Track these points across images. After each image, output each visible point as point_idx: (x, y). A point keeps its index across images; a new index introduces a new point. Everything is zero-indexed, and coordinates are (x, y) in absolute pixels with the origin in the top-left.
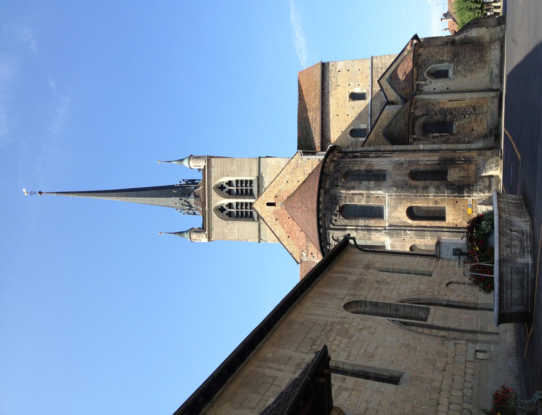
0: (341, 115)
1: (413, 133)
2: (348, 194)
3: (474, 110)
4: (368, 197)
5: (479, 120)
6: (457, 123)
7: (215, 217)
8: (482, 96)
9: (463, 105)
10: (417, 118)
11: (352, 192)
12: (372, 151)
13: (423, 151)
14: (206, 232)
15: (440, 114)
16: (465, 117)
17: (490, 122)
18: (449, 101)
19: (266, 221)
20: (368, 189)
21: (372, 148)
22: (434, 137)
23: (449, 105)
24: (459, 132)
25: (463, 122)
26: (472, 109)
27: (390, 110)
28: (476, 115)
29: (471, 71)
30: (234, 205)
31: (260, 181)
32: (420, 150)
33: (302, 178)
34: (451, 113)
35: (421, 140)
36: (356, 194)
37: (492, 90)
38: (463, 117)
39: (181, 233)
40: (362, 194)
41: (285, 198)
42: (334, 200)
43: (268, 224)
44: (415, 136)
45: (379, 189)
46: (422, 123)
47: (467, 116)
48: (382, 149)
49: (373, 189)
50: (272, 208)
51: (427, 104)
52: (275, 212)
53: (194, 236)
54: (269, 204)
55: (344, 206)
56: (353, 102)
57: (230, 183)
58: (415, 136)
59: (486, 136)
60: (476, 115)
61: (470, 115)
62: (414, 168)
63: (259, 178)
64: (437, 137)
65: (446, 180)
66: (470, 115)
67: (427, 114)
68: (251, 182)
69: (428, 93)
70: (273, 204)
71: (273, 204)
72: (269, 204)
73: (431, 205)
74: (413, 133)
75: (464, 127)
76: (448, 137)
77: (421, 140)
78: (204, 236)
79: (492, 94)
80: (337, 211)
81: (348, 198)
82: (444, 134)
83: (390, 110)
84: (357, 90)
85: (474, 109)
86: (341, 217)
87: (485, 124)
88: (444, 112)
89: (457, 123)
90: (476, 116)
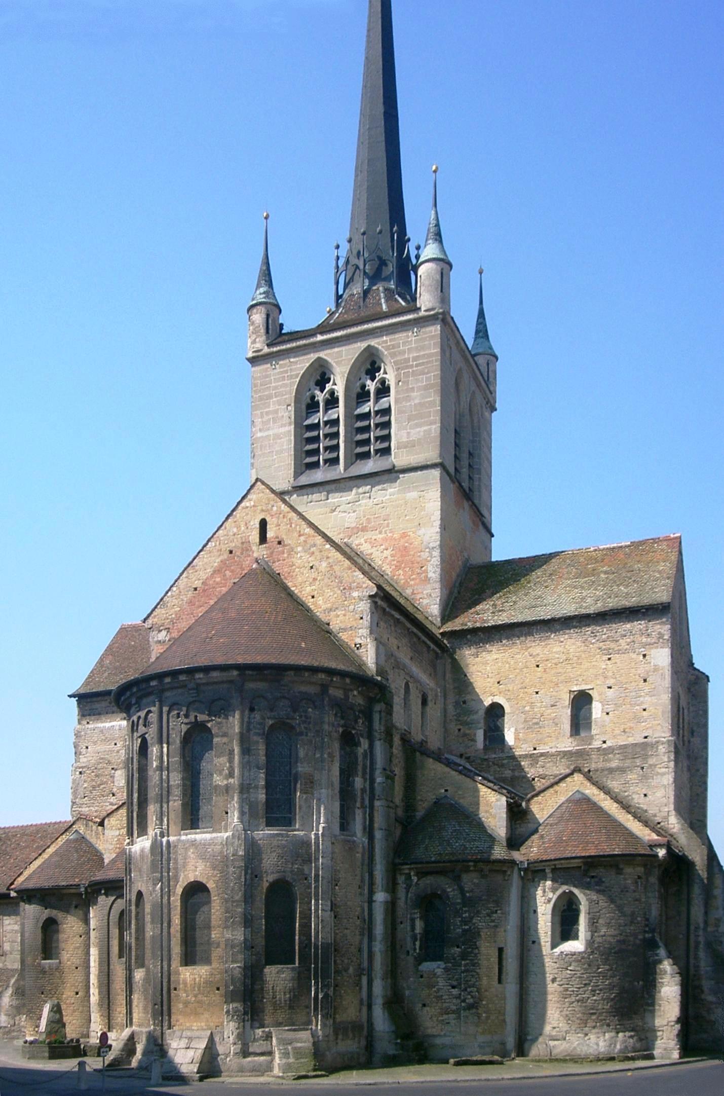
0: (539, 674)
1: (421, 874)
2: (231, 741)
4: (227, 788)
5: (445, 1017)
6: (439, 971)
7: (302, 364)
8: (508, 1020)
9: (485, 981)
10: (457, 879)
11: (237, 750)
12: (372, 781)
13: (371, 901)
14: (266, 350)
15: (464, 930)
16: (453, 987)
17: (438, 1041)
18: (501, 950)
19: (227, 524)
20: (244, 789)
21: (379, 780)
22: (413, 920)
23: (487, 952)
24: (422, 977)
25: (441, 982)
26: (471, 1001)
28: (457, 1012)
30: (332, 414)
31: (386, 477)
32: (371, 893)
34: (464, 956)
35: (407, 892)
36: (231, 761)
38: (455, 983)
41: (277, 567)
42: (219, 707)
43: (220, 532)
44: (415, 879)
45: (242, 813)
46: (444, 891)
47: (455, 992)
48: (377, 803)
49: (242, 801)
50: (255, 536)
52: (245, 546)
53: (258, 317)
55: (209, 730)
56: (567, 703)
58: (415, 879)
60: (457, 1012)
61: (458, 997)
62: (298, 890)
63: (392, 474)
64: (413, 928)
66: (458, 997)
67: (468, 902)
68: (386, 451)
70: (263, 539)
74: (421, 874)
75: (431, 986)
76: (411, 952)
77: (407, 892)
78: (258, 346)
80: (196, 717)
81: (225, 740)
82: (418, 943)
84: (597, 709)
85: (470, 1007)
86: (184, 728)
87: (434, 1031)
88: (470, 938)
89: (439, 971)
90: (453, 1012)
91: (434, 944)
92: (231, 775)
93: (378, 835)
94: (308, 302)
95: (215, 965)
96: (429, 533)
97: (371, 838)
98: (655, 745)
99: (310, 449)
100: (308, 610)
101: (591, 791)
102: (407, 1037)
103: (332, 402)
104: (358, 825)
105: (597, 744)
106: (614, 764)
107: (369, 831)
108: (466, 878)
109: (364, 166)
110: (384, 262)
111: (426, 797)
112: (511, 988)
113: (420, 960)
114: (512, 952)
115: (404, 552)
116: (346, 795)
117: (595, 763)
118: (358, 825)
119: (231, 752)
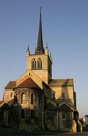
3: (53, 125)
10: (52, 111)
27: (55, 105)
29: (64, 124)
33: (36, 82)
37: (59, 129)
39: (28, 49)
40: (27, 99)
41: (31, 78)
51: (56, 114)
54: (30, 73)
57: (41, 61)
59: (46, 128)
63: (42, 69)
65: (31, 119)
67: (53, 114)
69: (59, 114)
70: (30, 75)
71: (30, 75)
72: (30, 73)
73: (25, 115)
79: (58, 129)
83: (55, 105)
91: (49, 118)
92: (27, 99)
93: (43, 106)
94: (33, 52)
95: (25, 119)
96: (47, 76)
97: (42, 106)
98: (72, 99)
99: (34, 67)
100: (35, 83)
101: (66, 103)
102: (46, 128)
103: (36, 62)
104: (41, 105)
105: (65, 99)
106: (67, 101)
107: (42, 106)
108: (53, 111)
109: (39, 38)
110: (41, 50)
111: (48, 103)
112: (58, 123)
113: (47, 120)
114: (58, 119)
115: (44, 78)
116: (39, 102)
117: (65, 101)
118: (41, 105)
119: (27, 96)
